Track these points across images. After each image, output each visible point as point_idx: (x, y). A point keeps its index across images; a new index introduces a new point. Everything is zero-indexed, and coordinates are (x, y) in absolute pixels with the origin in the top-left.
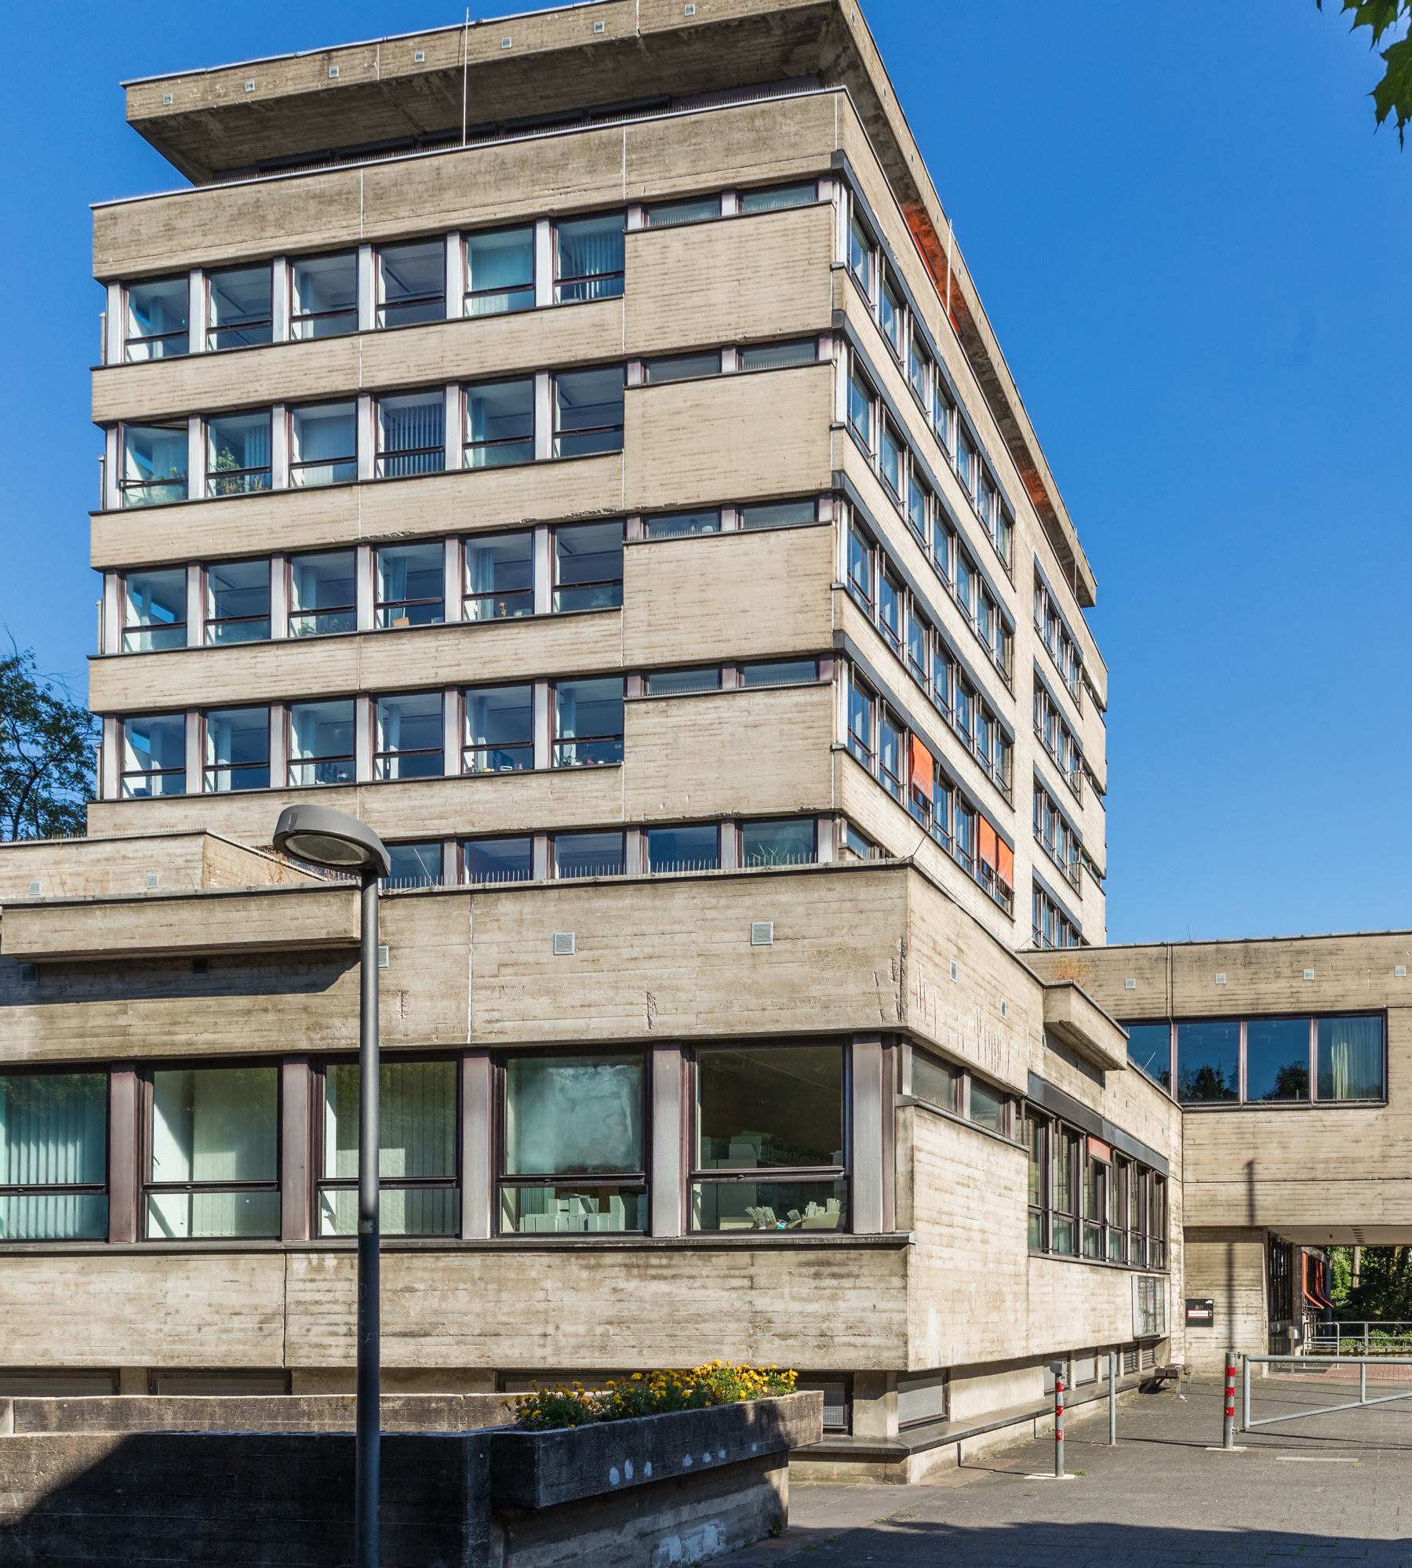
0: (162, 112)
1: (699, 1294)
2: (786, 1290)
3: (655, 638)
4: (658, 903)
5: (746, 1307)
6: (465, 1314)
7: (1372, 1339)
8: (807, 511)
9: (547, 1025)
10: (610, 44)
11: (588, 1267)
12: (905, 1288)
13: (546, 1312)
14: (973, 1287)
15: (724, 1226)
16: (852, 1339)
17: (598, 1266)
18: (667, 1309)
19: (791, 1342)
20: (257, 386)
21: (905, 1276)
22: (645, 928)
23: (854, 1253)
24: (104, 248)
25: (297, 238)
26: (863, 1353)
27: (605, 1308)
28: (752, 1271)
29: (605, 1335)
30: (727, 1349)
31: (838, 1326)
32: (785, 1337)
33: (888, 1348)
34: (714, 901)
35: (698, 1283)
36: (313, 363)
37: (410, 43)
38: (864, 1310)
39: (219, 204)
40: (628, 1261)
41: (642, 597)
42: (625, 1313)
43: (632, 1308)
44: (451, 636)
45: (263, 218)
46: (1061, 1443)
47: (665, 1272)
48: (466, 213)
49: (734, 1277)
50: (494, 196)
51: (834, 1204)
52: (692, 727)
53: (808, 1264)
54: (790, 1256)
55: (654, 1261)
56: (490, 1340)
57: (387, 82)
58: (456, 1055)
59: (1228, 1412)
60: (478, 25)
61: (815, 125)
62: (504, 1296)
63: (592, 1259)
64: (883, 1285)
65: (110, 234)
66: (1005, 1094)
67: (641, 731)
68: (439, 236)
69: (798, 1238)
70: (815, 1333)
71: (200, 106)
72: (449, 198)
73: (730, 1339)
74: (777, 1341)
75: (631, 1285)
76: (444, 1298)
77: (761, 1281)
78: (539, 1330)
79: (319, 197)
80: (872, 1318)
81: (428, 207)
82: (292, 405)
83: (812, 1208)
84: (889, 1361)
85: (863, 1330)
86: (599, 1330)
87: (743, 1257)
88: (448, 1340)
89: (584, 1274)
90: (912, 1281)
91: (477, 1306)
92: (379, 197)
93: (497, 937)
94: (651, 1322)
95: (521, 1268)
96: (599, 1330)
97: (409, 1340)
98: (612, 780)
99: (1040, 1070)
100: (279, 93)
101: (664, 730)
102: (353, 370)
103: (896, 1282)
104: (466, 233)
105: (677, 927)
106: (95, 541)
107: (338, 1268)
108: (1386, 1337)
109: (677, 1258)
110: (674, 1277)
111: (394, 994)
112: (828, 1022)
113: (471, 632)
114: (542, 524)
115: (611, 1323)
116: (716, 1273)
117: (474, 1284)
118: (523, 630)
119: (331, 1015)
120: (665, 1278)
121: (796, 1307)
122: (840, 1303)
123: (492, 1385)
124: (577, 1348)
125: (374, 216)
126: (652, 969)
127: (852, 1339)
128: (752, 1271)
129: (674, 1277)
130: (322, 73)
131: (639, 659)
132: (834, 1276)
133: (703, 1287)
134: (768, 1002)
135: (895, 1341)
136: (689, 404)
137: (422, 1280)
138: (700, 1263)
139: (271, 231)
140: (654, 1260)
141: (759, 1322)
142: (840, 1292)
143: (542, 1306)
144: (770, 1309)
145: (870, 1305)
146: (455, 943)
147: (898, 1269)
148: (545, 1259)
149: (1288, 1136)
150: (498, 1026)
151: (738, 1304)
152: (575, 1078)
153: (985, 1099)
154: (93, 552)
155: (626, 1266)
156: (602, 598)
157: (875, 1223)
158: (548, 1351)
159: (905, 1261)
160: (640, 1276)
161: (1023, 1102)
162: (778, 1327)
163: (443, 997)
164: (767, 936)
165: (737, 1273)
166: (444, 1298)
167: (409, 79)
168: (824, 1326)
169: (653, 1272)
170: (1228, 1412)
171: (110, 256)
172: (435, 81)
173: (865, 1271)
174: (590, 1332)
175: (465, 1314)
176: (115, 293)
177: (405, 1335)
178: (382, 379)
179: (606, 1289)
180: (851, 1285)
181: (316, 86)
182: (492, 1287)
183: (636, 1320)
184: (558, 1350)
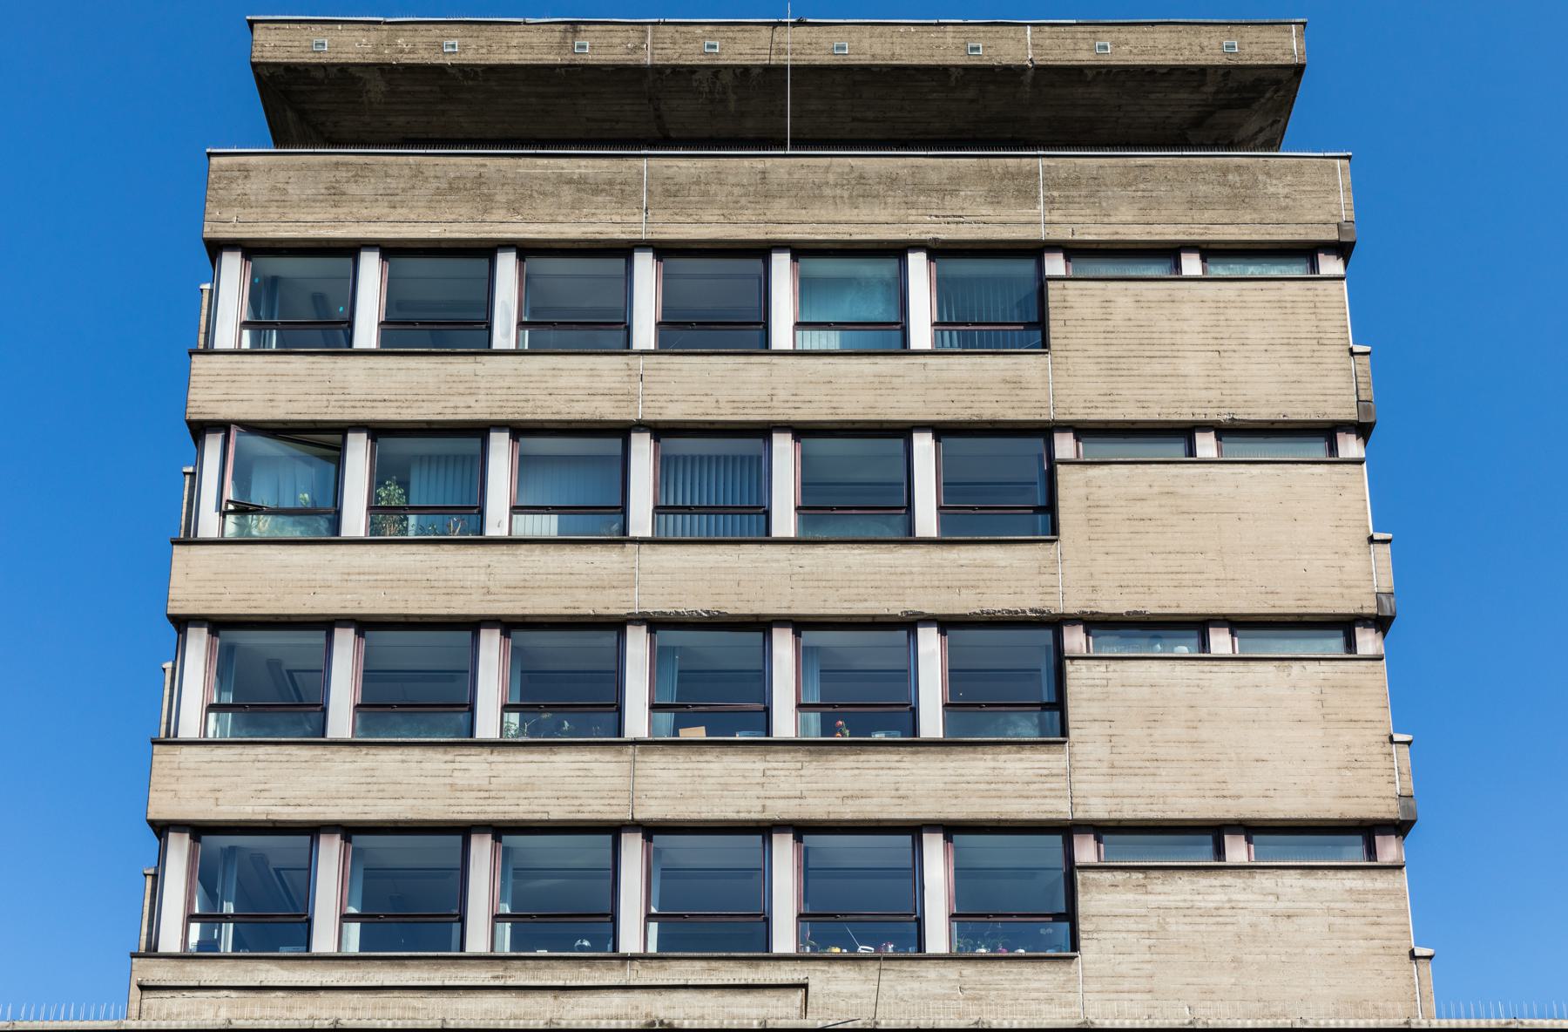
0: (309, 58)
3: (1120, 785)
10: (991, 69)
20: (471, 401)
24: (220, 203)
25: (542, 227)
36: (563, 382)
37: (698, 30)
39: (418, 172)
41: (1096, 729)
44: (787, 757)
45: (489, 198)
48: (807, 228)
50: (847, 213)
52: (1187, 911)
57: (658, 70)
60: (800, 23)
61: (1304, 189)
65: (237, 189)
67: (1106, 911)
68: (762, 251)
71: (371, 59)
72: (779, 208)
79: (580, 183)
81: (748, 214)
82: (518, 430)
92: (672, 193)
98: (1061, 977)
100: (494, 59)
101: (1144, 911)
102: (630, 397)
104: (800, 251)
106: (177, 578)
113: (821, 753)
114: (929, 620)
118: (908, 758)
125: (662, 216)
130: (562, 45)
131: (1098, 810)
136: (1156, 490)
139: (499, 214)
154: (173, 594)
156: (1026, 727)
167: (692, 70)
171: (231, 214)
172: (726, 78)
176: (232, 263)
178: (674, 412)
181: (552, 58)
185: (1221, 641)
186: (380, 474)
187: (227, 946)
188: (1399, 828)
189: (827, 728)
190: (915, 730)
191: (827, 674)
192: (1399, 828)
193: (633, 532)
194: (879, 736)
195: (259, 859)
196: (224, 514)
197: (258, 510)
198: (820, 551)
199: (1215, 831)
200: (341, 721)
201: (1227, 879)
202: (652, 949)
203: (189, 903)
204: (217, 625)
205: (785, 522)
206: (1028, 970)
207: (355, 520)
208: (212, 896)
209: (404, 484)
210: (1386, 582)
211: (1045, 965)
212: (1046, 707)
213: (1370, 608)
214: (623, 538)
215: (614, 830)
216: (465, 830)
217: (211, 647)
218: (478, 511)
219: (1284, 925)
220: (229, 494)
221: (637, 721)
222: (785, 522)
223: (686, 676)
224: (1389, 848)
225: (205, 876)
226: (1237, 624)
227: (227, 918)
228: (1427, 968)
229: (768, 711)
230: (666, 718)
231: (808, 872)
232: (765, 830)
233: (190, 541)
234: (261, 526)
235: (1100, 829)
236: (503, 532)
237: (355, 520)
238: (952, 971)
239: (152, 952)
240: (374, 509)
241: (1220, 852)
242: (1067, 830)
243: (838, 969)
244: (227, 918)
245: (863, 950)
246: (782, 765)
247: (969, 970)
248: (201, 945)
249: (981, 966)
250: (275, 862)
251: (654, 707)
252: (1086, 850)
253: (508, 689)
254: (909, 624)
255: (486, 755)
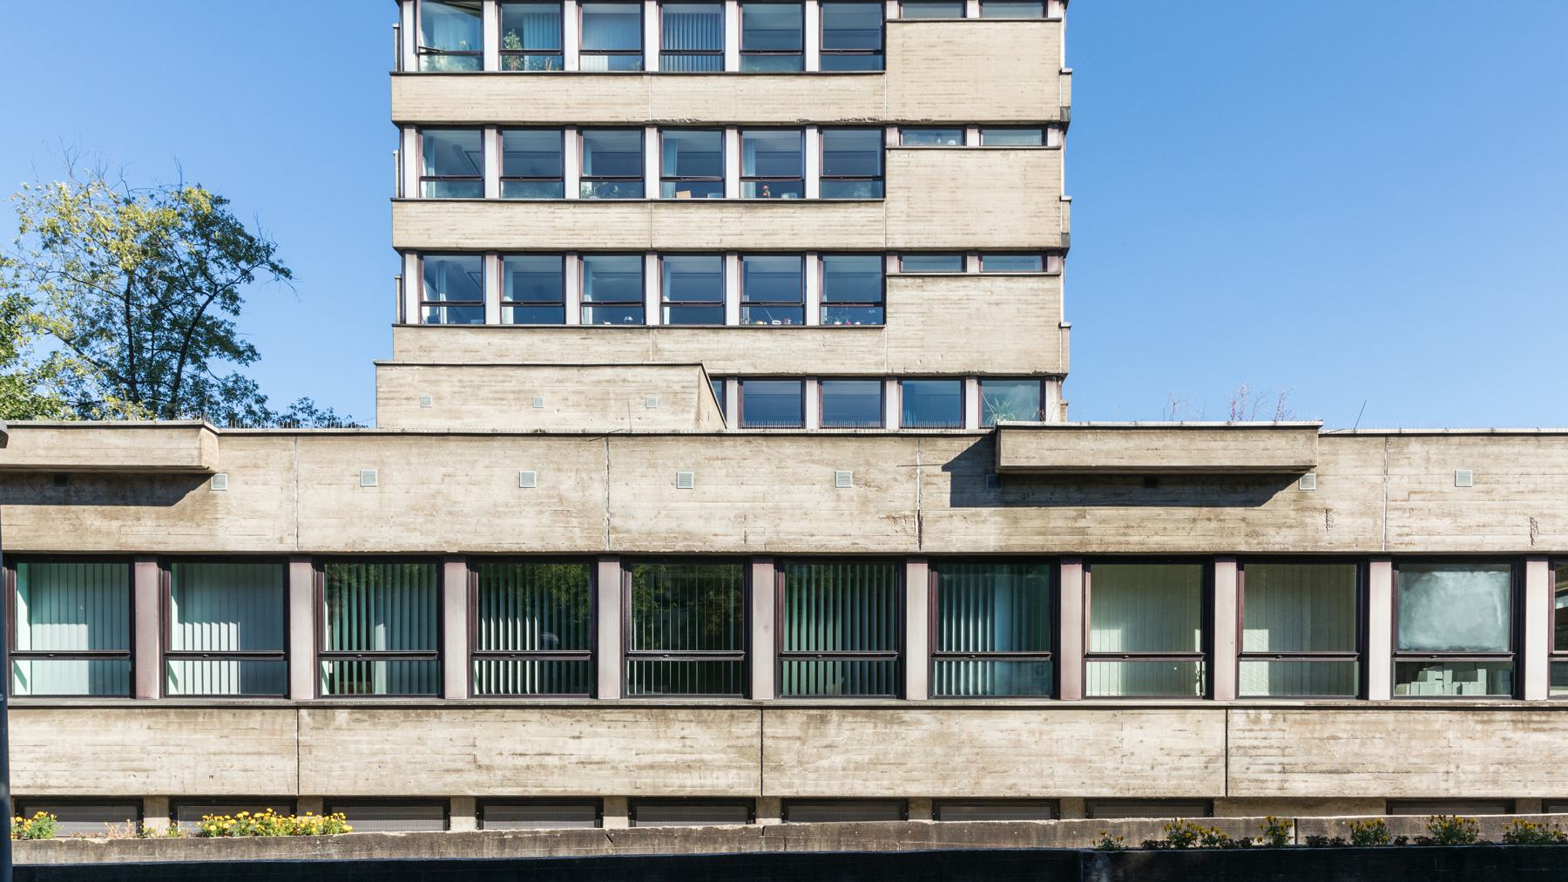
4: (1540, 451)
8: (1036, 138)
22: (1530, 470)
41: (901, 193)
47: (1545, 726)
52: (943, 301)
91: (1391, 751)
95: (1427, 722)
97: (1334, 776)
105: (1556, 470)
107: (1273, 721)
111: (1320, 511)
114: (812, 125)
117: (1389, 734)
119: (1267, 525)
123: (929, 812)
126: (1535, 501)
131: (899, 242)
137: (1345, 731)
143: (1447, 750)
146: (1373, 474)
148: (1447, 715)
150: (1407, 539)
156: (864, 191)
158: (1451, 784)
163: (1362, 514)
174: (1485, 771)
177: (1331, 772)
184: (1458, 783)
185: (973, 138)
186: (506, 27)
187: (444, 320)
188: (1061, 252)
189: (759, 194)
190: (803, 195)
191: (759, 154)
192: (1061, 252)
193: (648, 69)
194: (785, 197)
195: (458, 267)
196: (418, 55)
197: (438, 53)
198: (752, 80)
199: (963, 254)
200: (493, 188)
201: (966, 282)
202: (667, 322)
203: (421, 295)
204: (421, 127)
205: (733, 61)
206: (859, 335)
207: (492, 61)
208: (434, 289)
209: (520, 33)
210: (1066, 100)
211: (868, 332)
212: (875, 178)
213: (1056, 117)
214: (642, 73)
215: (642, 253)
216: (563, 253)
217: (418, 141)
218: (560, 53)
219: (994, 309)
220: (422, 42)
221: (653, 188)
222: (733, 61)
223: (682, 156)
224: (1054, 264)
225: (428, 276)
226: (982, 126)
227: (442, 304)
228: (1067, 333)
229: (724, 181)
230: (671, 185)
231: (746, 275)
232: (723, 253)
233: (400, 73)
234: (443, 62)
235: (901, 253)
236: (575, 69)
237: (492, 61)
238: (819, 335)
239: (403, 323)
240: (502, 52)
241: (964, 267)
242: (884, 253)
243: (761, 335)
244: (442, 304)
245: (776, 323)
246: (731, 213)
247: (828, 335)
248: (430, 319)
249: (834, 333)
250: (467, 269)
251: (662, 179)
252: (893, 266)
253: (583, 168)
254: (802, 127)
255: (570, 209)
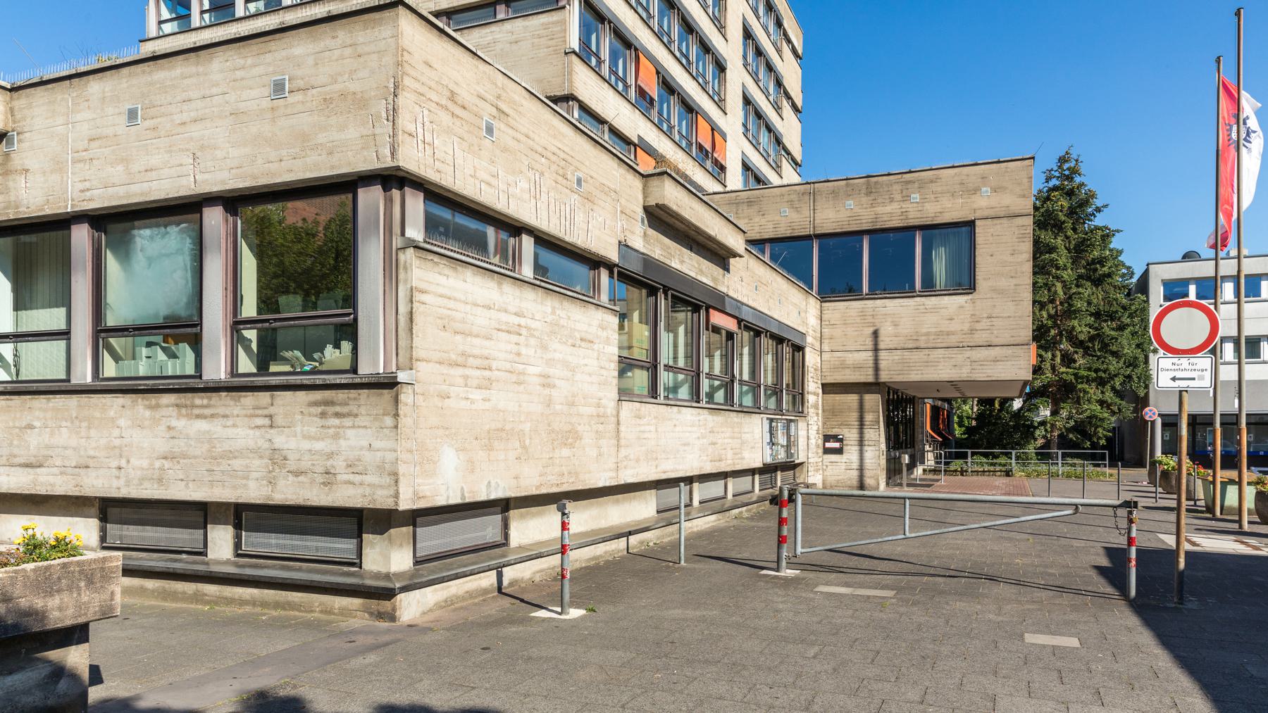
1: (231, 432)
2: (298, 429)
5: (267, 445)
6: (65, 448)
7: (972, 463)
9: (121, 191)
11: (150, 407)
12: (396, 427)
13: (120, 448)
14: (527, 427)
15: (274, 368)
16: (351, 477)
17: (158, 406)
18: (206, 446)
19: (301, 478)
21: (396, 415)
23: (353, 393)
26: (360, 491)
27: (162, 446)
28: (272, 410)
29: (162, 469)
30: (252, 484)
31: (339, 464)
32: (297, 473)
33: (381, 487)
34: (242, 62)
35: (230, 423)
38: (361, 449)
40: (178, 402)
42: (176, 450)
43: (180, 445)
46: (566, 582)
49: (257, 416)
51: (346, 346)
53: (316, 404)
54: (301, 395)
55: (198, 402)
56: (82, 471)
58: (62, 223)
59: (781, 540)
62: (93, 433)
63: (153, 399)
64: (377, 424)
66: (594, 262)
69: (319, 379)
70: (321, 470)
73: (254, 475)
74: (291, 478)
75: (180, 424)
76: (52, 434)
77: (279, 420)
78: (114, 464)
80: (367, 456)
83: (329, 349)
84: (382, 500)
85: (360, 469)
86: (158, 464)
87: (264, 397)
88: (55, 470)
89: (148, 413)
90: (405, 421)
93: (87, 115)
94: (195, 457)
96: (158, 464)
99: (638, 243)
103: (389, 421)
108: (985, 460)
109: (215, 398)
110: (212, 416)
112: (332, 167)
115: (165, 458)
116: (244, 412)
120: (205, 417)
121: (306, 445)
122: (342, 442)
124: (142, 479)
127: (351, 477)
128: (272, 410)
129: (212, 416)
132: (337, 415)
133: (234, 426)
134: (284, 153)
135: (387, 480)
138: (232, 403)
140: (199, 399)
141: (277, 458)
142: (341, 431)
144: (286, 447)
145: (366, 444)
147: (391, 408)
149: (899, 316)
151: (261, 442)
152: (152, 238)
153: (549, 257)
155: (177, 405)
157: (376, 363)
159: (396, 400)
160: (187, 415)
161: (616, 270)
162: (292, 465)
164: (283, 89)
165: (260, 412)
166: (52, 434)
168: (329, 463)
169: (196, 411)
170: (781, 540)
173: (363, 410)
175: (65, 448)
179: (163, 428)
180: (350, 424)
182: (84, 424)
183: (185, 456)
